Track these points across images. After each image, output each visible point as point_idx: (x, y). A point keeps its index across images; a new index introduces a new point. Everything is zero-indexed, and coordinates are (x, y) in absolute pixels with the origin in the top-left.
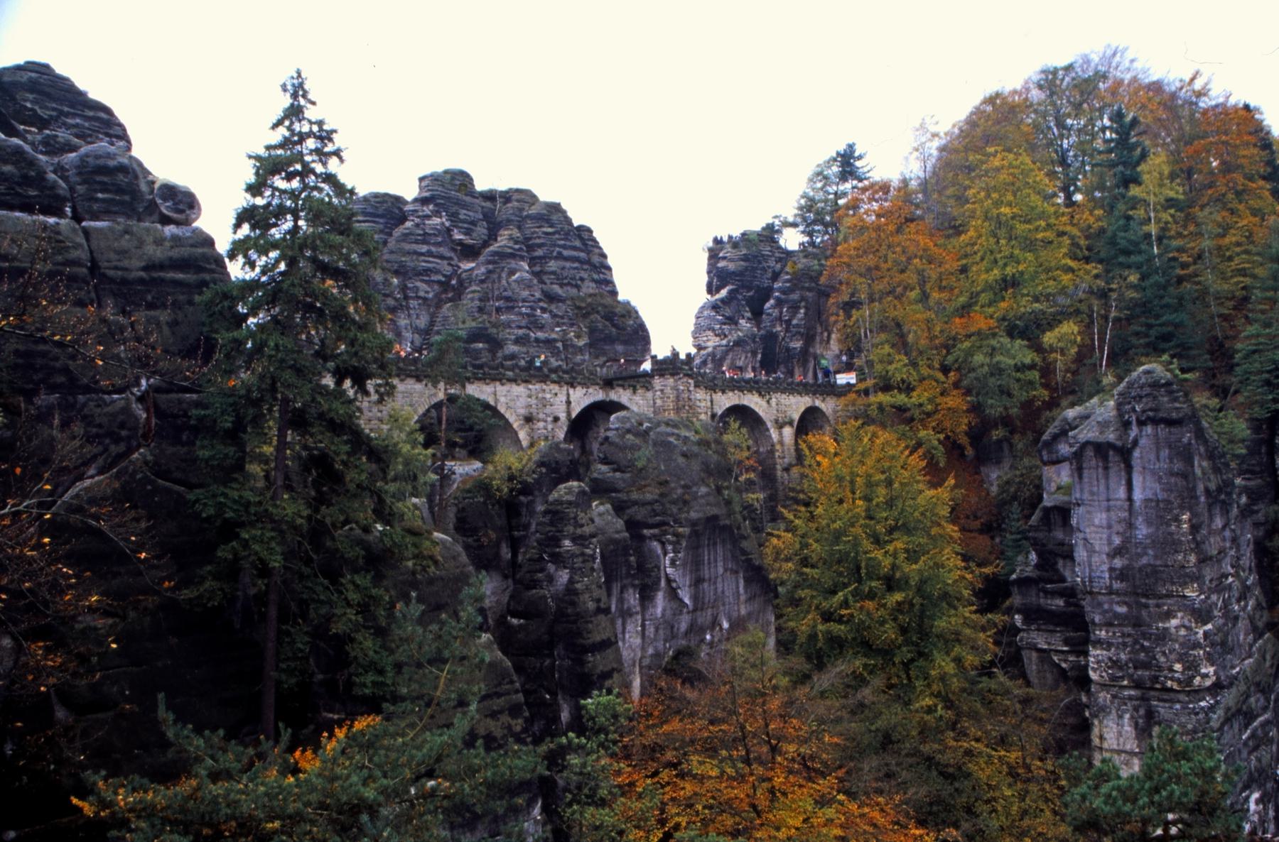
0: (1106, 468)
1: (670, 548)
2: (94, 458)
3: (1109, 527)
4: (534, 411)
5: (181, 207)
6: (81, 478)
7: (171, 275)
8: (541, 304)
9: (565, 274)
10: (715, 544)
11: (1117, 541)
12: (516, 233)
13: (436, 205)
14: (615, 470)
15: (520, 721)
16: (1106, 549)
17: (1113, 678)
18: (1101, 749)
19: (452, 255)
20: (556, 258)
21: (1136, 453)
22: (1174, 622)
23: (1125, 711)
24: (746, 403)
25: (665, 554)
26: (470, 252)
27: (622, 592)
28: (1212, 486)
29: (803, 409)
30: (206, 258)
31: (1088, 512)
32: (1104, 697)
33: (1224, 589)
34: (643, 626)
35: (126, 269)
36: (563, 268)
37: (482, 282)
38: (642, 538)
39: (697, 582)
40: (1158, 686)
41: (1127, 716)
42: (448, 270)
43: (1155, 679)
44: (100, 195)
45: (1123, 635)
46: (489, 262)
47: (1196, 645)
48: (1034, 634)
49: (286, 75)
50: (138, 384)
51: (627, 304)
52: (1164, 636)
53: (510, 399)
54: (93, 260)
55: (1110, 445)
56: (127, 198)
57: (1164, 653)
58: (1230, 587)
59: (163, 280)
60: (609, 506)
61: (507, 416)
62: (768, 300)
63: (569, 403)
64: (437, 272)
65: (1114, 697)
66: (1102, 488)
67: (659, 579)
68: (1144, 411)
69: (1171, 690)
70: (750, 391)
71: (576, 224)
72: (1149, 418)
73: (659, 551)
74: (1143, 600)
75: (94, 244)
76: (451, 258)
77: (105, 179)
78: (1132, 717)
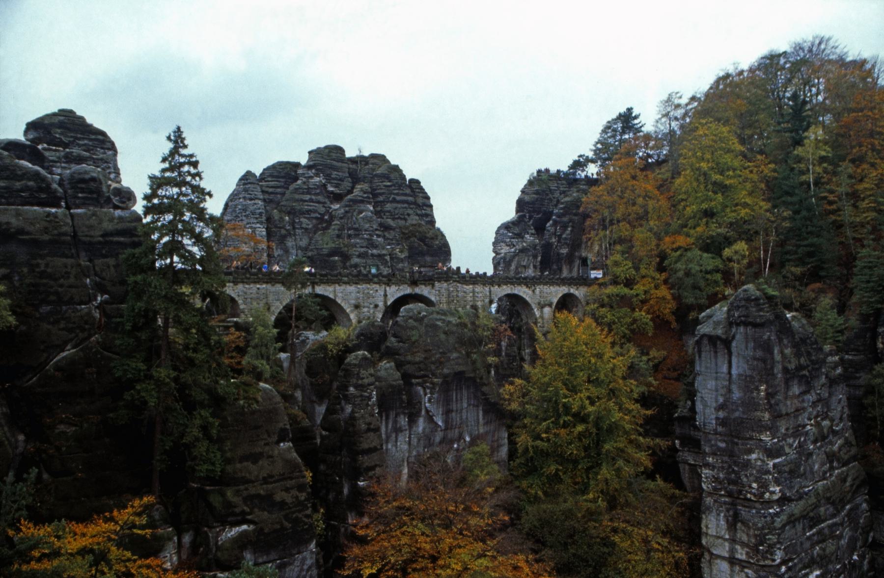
0: (716, 352)
1: (428, 391)
2: (71, 340)
3: (717, 390)
4: (360, 301)
5: (124, 200)
6: (63, 351)
7: (116, 239)
8: (377, 232)
9: (397, 212)
10: (461, 389)
11: (721, 400)
13: (317, 170)
14: (399, 342)
15: (304, 494)
16: (714, 405)
17: (715, 489)
18: (707, 534)
19: (326, 200)
20: (391, 202)
21: (734, 344)
22: (754, 456)
23: (721, 512)
24: (516, 292)
25: (426, 394)
26: (337, 198)
27: (396, 417)
28: (791, 366)
29: (560, 295)
30: (135, 228)
31: (705, 380)
32: (709, 500)
33: (800, 435)
34: (410, 438)
35: (91, 236)
36: (396, 208)
37: (341, 218)
38: (412, 384)
39: (447, 412)
40: (742, 497)
41: (722, 515)
43: (740, 492)
44: (80, 195)
45: (722, 462)
46: (347, 206)
47: (768, 472)
48: (686, 454)
49: (170, 130)
50: (96, 300)
52: (747, 464)
53: (343, 294)
54: (75, 232)
55: (718, 338)
56: (95, 196)
57: (746, 476)
58: (807, 433)
59: (112, 242)
60: (393, 364)
61: (343, 305)
62: (549, 221)
63: (385, 295)
64: (315, 211)
65: (715, 501)
66: (713, 365)
67: (421, 410)
68: (739, 317)
69: (750, 500)
70: (519, 284)
71: (408, 178)
72: (741, 322)
73: (422, 393)
74: (736, 440)
75: (76, 222)
76: (325, 203)
77: (83, 186)
78: (725, 516)
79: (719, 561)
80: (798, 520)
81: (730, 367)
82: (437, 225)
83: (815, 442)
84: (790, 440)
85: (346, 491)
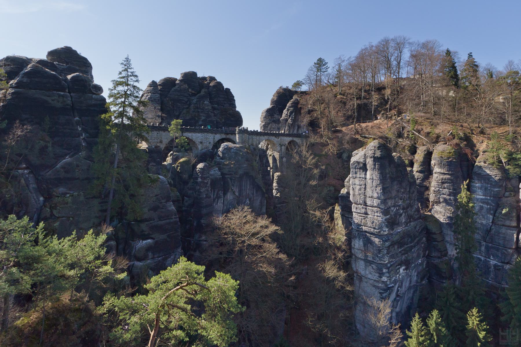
12: (206, 90)
34: (224, 201)
39: (240, 191)
50: (82, 136)
51: (238, 111)
71: (225, 87)
73: (230, 181)
79: (359, 260)
80: (395, 244)
81: (366, 174)
82: (237, 109)
83: (403, 209)
84: (393, 208)
85: (195, 224)
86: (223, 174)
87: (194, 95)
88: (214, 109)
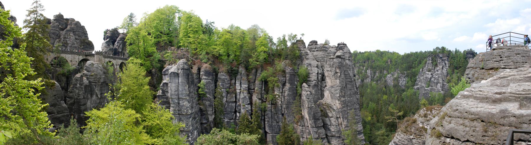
39: (101, 94)
42: (58, 33)
86: (90, 82)
87: (63, 30)
88: (76, 39)
